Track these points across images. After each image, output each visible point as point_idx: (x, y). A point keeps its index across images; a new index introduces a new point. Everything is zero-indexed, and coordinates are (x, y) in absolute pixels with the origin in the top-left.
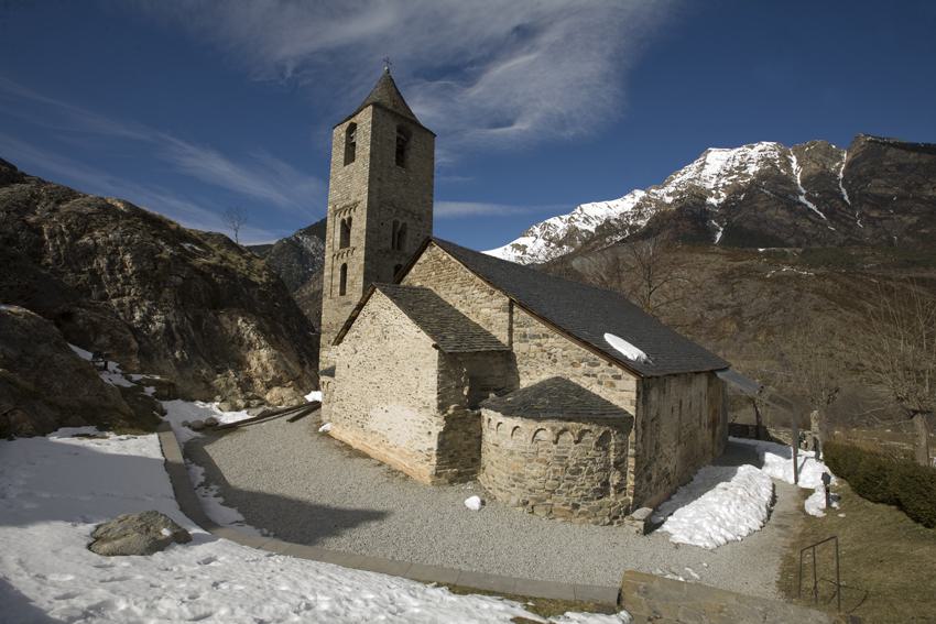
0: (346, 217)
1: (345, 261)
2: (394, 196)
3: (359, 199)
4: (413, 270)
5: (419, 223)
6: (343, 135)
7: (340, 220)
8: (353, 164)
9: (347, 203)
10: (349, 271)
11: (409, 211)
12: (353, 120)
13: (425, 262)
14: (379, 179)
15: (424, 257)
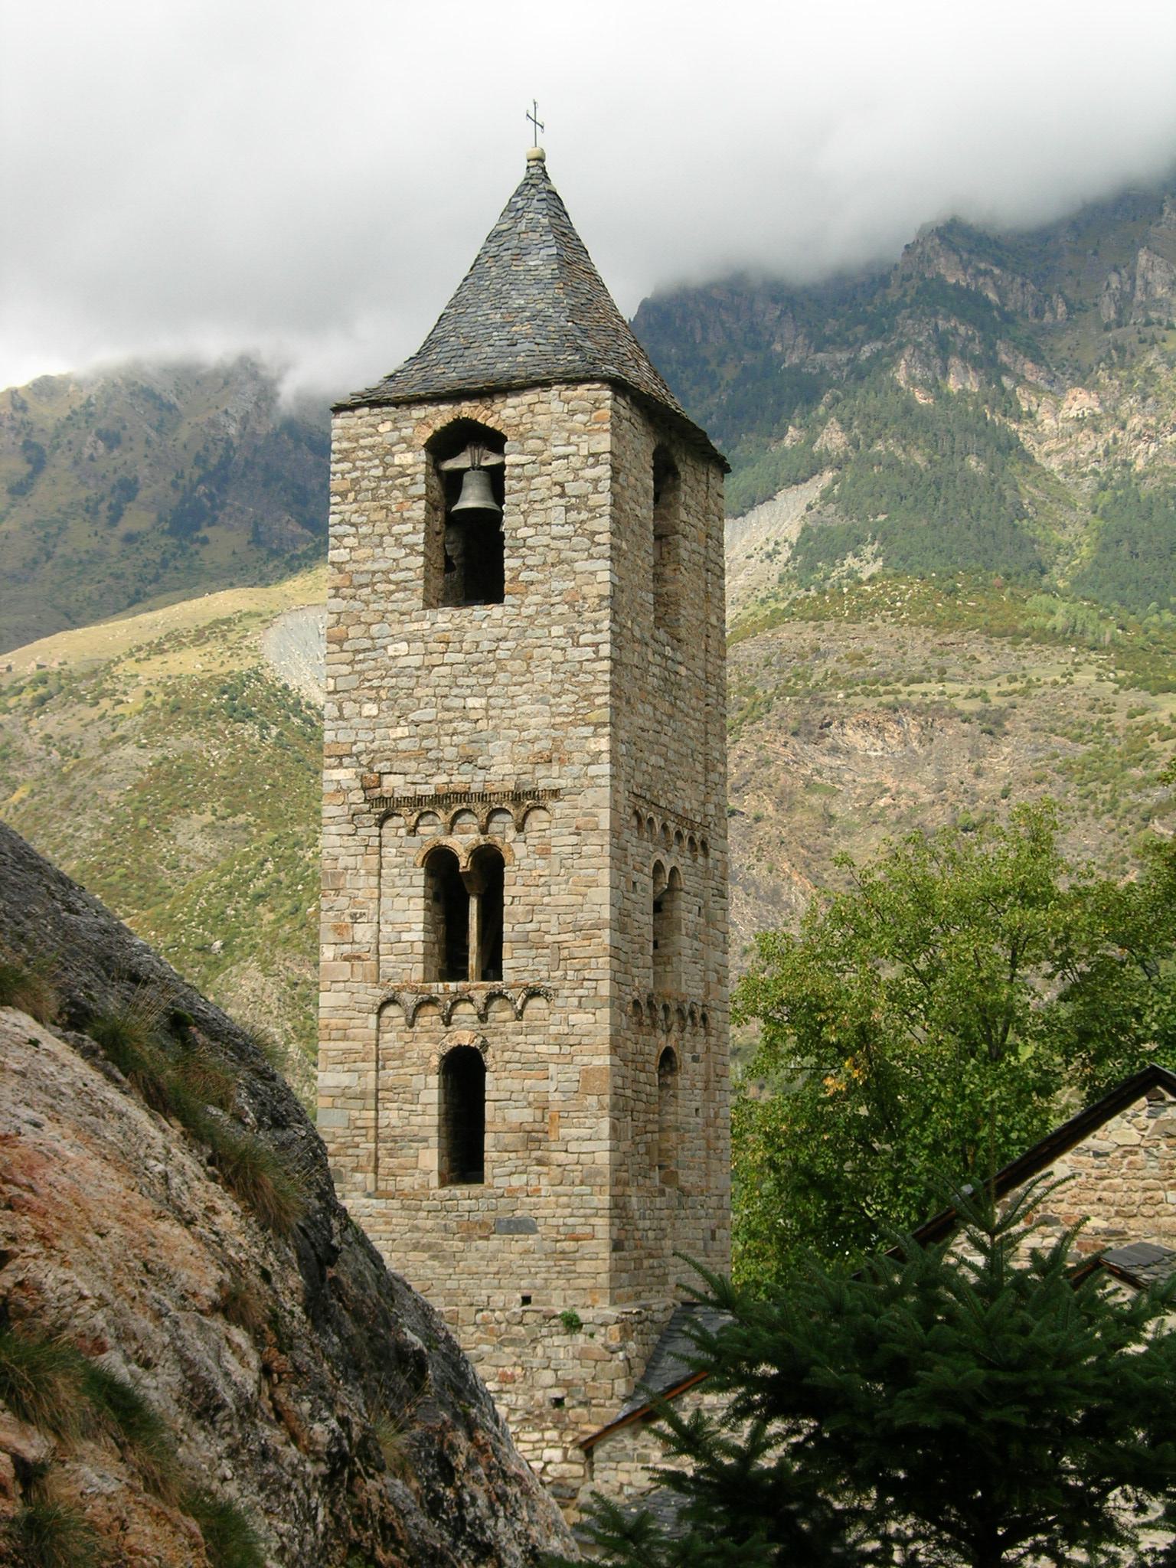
0: (462, 843)
1: (464, 1036)
2: (653, 760)
3: (546, 778)
4: (1060, 1167)
5: (701, 860)
6: (413, 460)
7: (416, 850)
8: (496, 611)
9: (461, 779)
10: (493, 1085)
11: (681, 819)
12: (467, 410)
13: (1130, 1151)
14: (628, 702)
15: (1118, 1131)
